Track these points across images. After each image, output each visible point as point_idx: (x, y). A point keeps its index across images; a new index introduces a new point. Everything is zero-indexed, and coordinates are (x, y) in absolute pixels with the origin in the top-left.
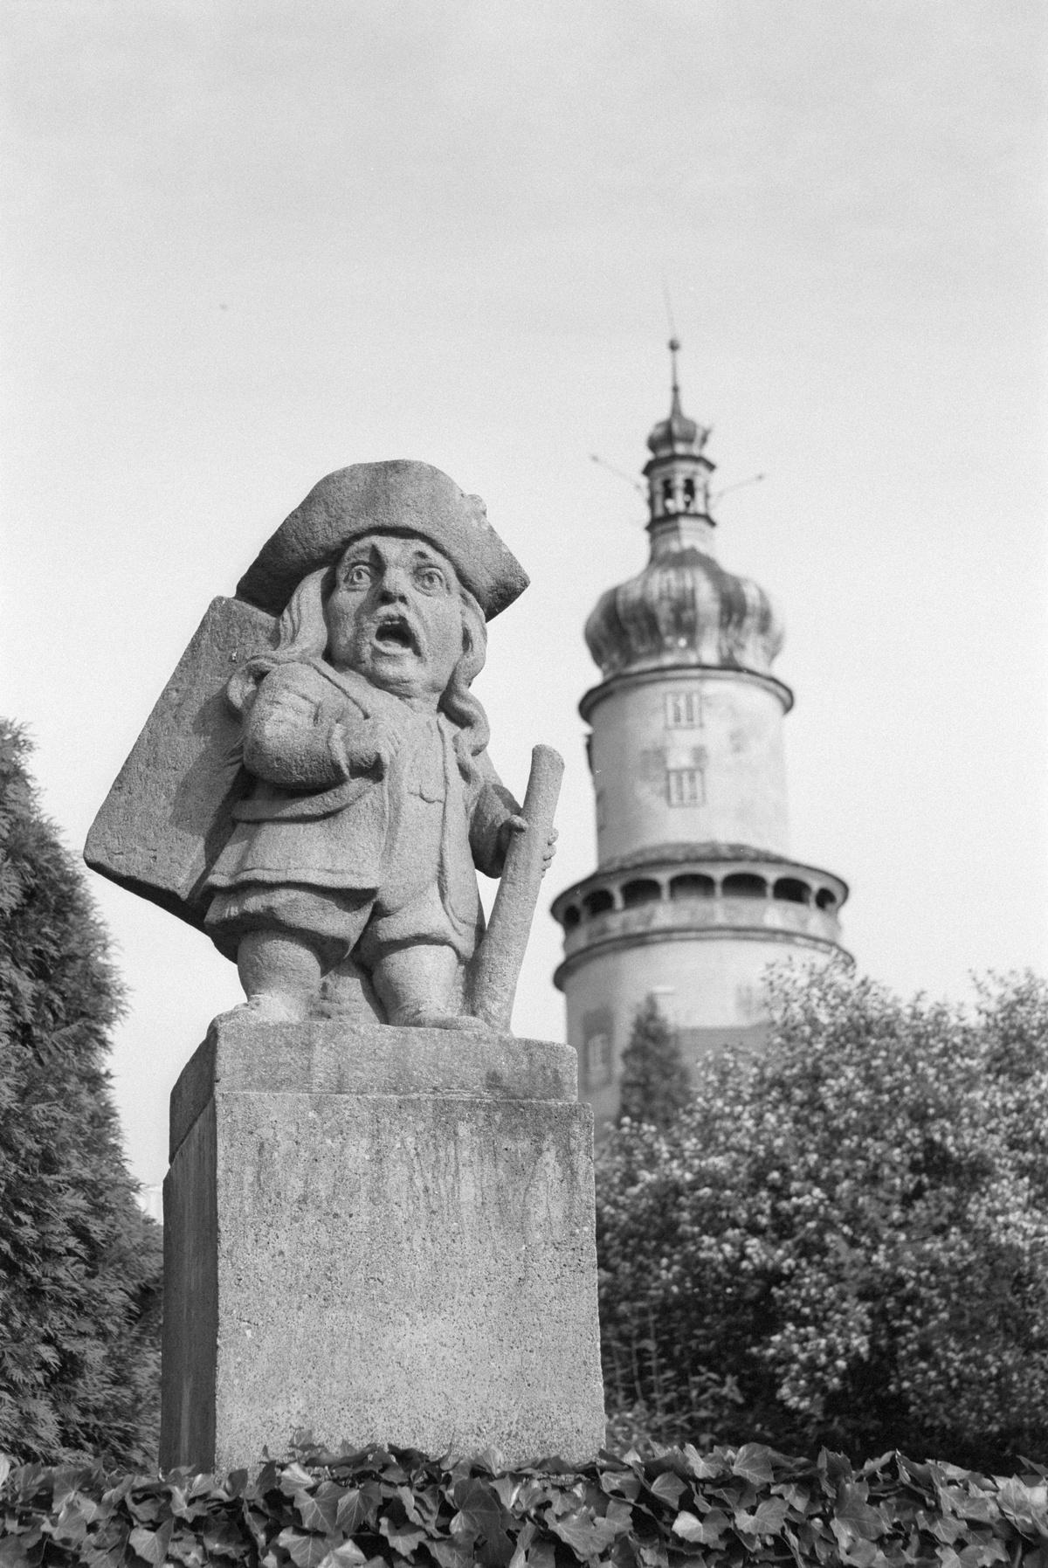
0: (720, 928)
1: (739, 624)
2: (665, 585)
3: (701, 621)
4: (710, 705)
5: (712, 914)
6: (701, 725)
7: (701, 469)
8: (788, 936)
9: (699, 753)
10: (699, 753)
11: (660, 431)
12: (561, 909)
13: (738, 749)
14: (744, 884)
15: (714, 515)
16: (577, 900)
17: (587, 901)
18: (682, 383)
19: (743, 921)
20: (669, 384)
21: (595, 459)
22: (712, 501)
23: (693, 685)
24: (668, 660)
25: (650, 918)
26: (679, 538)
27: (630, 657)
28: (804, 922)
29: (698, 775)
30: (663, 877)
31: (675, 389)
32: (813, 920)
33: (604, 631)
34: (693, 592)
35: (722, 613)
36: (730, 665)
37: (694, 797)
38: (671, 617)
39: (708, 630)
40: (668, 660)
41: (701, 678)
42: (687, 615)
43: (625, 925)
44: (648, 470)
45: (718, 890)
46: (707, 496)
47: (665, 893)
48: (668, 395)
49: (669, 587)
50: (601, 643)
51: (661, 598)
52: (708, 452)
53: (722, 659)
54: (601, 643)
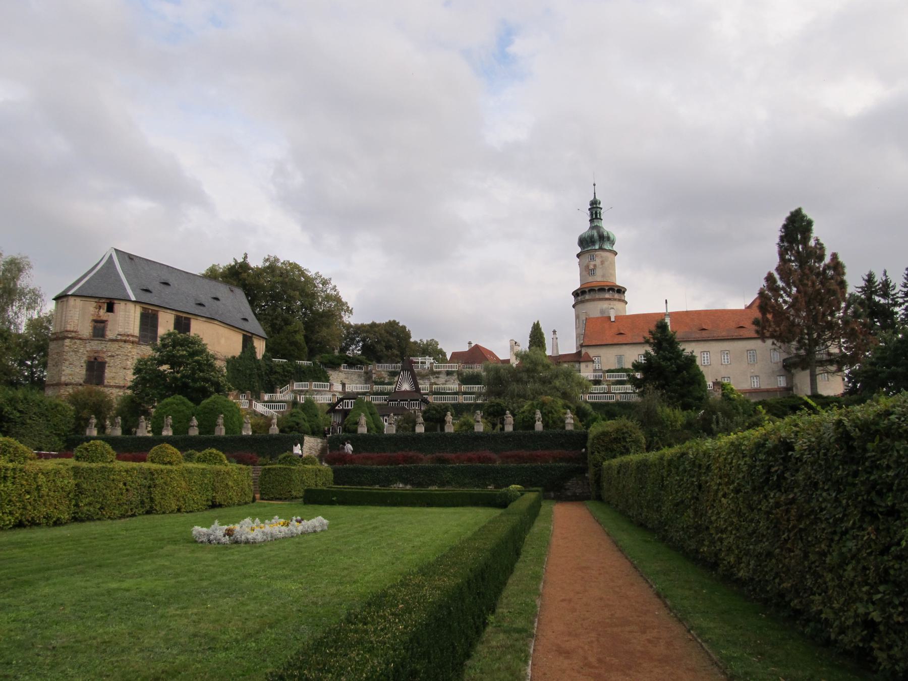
8: (610, 299)
9: (595, 266)
14: (602, 290)
19: (601, 297)
24: (589, 248)
25: (584, 298)
28: (614, 296)
30: (587, 290)
31: (595, 193)
32: (616, 296)
36: (601, 249)
40: (589, 248)
42: (593, 240)
52: (601, 206)
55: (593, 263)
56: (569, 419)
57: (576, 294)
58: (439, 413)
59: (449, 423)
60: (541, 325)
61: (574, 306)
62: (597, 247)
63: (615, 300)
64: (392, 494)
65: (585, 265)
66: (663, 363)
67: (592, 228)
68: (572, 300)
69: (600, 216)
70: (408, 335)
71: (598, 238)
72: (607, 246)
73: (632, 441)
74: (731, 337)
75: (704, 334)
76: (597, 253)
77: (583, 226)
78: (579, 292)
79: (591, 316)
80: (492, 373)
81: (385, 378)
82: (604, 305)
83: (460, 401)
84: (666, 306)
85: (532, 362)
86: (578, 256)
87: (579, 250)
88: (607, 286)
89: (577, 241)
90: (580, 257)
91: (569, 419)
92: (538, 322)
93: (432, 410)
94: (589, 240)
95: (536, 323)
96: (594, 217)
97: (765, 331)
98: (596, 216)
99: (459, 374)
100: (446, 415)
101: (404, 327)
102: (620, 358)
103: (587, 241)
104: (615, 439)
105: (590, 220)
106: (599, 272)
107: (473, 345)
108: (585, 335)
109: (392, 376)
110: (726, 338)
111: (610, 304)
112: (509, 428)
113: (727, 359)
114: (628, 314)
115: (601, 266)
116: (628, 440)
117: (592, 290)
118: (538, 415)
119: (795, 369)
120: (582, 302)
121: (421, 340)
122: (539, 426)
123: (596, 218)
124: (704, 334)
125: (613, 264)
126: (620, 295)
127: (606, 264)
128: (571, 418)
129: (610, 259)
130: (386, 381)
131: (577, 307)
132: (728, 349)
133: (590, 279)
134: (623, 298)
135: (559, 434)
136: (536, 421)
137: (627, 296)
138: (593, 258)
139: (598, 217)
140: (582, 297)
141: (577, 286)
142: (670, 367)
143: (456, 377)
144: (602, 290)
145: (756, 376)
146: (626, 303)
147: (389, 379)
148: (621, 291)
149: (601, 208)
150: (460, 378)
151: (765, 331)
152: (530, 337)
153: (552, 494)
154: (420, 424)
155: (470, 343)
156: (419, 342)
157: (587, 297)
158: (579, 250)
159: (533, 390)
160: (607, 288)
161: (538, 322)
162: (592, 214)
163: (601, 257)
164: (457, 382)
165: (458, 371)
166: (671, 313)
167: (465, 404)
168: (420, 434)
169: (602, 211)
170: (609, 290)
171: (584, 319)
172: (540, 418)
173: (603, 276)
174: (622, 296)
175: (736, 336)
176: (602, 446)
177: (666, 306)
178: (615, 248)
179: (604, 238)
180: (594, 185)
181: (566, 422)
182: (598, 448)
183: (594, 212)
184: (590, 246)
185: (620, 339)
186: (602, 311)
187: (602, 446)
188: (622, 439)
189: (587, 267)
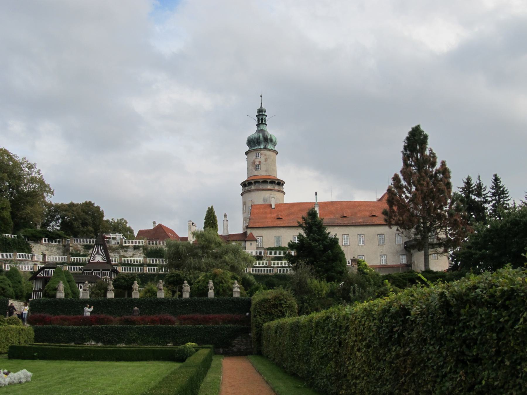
0: (261, 189)
1: (267, 141)
7: (264, 116)
8: (271, 190)
9: (260, 162)
10: (260, 162)
13: (266, 161)
14: (265, 182)
15: (267, 124)
16: (243, 185)
17: (244, 185)
18: (262, 102)
19: (264, 188)
22: (266, 121)
23: (259, 152)
24: (256, 148)
25: (251, 187)
27: (251, 147)
30: (253, 182)
31: (261, 103)
32: (277, 187)
36: (265, 148)
37: (259, 169)
39: (262, 143)
40: (256, 148)
41: (261, 151)
42: (258, 141)
52: (266, 114)
53: (264, 147)
55: (258, 160)
56: (236, 288)
57: (244, 185)
58: (127, 281)
59: (136, 290)
60: (214, 210)
61: (242, 195)
62: (262, 147)
63: (276, 190)
64: (87, 351)
66: (313, 244)
67: (258, 131)
68: (240, 190)
69: (265, 122)
70: (101, 215)
72: (270, 147)
73: (287, 307)
74: (366, 224)
75: (345, 221)
76: (262, 152)
77: (252, 130)
78: (246, 183)
79: (256, 203)
80: (173, 249)
81: (80, 251)
82: (267, 195)
83: (145, 272)
84: (316, 197)
85: (206, 240)
86: (247, 153)
87: (247, 148)
88: (269, 179)
89: (246, 141)
90: (248, 155)
91: (236, 288)
92: (212, 207)
93: (121, 279)
94: (255, 141)
95: (210, 207)
96: (260, 122)
97: (392, 220)
98: (262, 121)
99: (145, 248)
100: (133, 283)
101: (98, 208)
102: (278, 238)
103: (254, 141)
104: (273, 305)
105: (257, 125)
106: (263, 167)
107: (157, 225)
108: (250, 219)
109: (87, 249)
110: (362, 224)
111: (271, 194)
112: (186, 295)
113: (363, 241)
114: (285, 202)
115: (264, 163)
116: (284, 306)
117: (257, 182)
118: (211, 284)
119: (414, 250)
120: (249, 191)
121: (112, 219)
122: (211, 294)
123: (262, 123)
124: (345, 221)
125: (274, 161)
126: (279, 187)
127: (269, 161)
128: (238, 287)
130: (81, 254)
131: (244, 195)
132: (363, 233)
133: (256, 173)
134: (282, 190)
135: (228, 300)
136: (209, 290)
137: (285, 188)
138: (258, 156)
139: (264, 122)
140: (249, 187)
141: (245, 178)
142: (318, 247)
143: (142, 251)
144: (265, 182)
145: (384, 255)
146: (284, 193)
147: (84, 251)
148: (280, 183)
149: (266, 116)
150: (145, 252)
151: (392, 220)
152: (205, 219)
153: (221, 350)
154: (111, 290)
155: (154, 223)
156: (111, 220)
157: (253, 187)
158: (247, 148)
159: (207, 263)
160: (269, 181)
161: (212, 207)
162: (258, 120)
164: (143, 255)
165: (143, 246)
166: (319, 203)
167: (149, 274)
168: (111, 299)
169: (267, 118)
171: (250, 205)
172: (212, 287)
173: (266, 171)
174: (281, 187)
175: (370, 223)
176: (263, 310)
177: (316, 197)
178: (276, 149)
179: (267, 140)
180: (261, 96)
181: (234, 290)
182: (260, 312)
183: (260, 118)
184: (256, 146)
185: (279, 223)
186: (265, 200)
187: (263, 310)
188: (279, 305)
189: (254, 162)
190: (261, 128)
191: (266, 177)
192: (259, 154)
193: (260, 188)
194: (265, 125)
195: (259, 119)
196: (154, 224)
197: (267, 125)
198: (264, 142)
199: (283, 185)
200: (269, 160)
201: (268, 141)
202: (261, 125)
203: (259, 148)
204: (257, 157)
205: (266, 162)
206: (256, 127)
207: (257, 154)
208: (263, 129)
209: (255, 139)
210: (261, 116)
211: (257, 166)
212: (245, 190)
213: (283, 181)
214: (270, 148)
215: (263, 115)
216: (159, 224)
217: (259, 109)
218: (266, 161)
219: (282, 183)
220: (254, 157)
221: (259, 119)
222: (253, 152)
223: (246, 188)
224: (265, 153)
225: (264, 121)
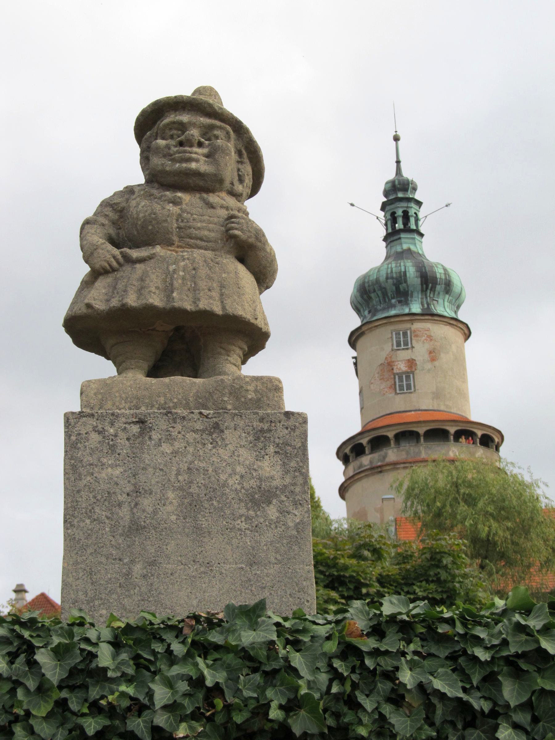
1: (433, 289)
2: (389, 271)
3: (411, 289)
4: (416, 336)
5: (420, 452)
6: (413, 347)
7: (412, 205)
9: (411, 363)
11: (389, 185)
12: (341, 455)
15: (422, 230)
16: (347, 450)
17: (353, 449)
18: (401, 159)
20: (395, 159)
21: (352, 205)
22: (420, 223)
23: (408, 325)
25: (385, 457)
26: (401, 244)
27: (374, 312)
28: (473, 454)
29: (411, 375)
30: (391, 434)
31: (398, 162)
33: (359, 299)
34: (405, 273)
35: (422, 284)
37: (409, 387)
38: (394, 288)
39: (415, 294)
40: (393, 312)
41: (412, 321)
42: (402, 287)
43: (371, 462)
44: (384, 207)
45: (422, 439)
46: (417, 220)
47: (392, 442)
48: (395, 165)
49: (392, 272)
50: (359, 306)
51: (387, 278)
54: (359, 306)
55: (404, 355)
65: (381, 360)
69: (417, 224)
71: (418, 281)
76: (417, 326)
88: (454, 422)
94: (390, 286)
96: (399, 225)
107: (29, 597)
115: (429, 366)
123: (407, 229)
125: (460, 360)
127: (445, 359)
129: (454, 347)
131: (356, 489)
149: (419, 204)
158: (355, 322)
160: (452, 430)
162: (393, 219)
163: (430, 338)
170: (458, 435)
180: (396, 139)
183: (399, 213)
184: (393, 306)
189: (389, 365)
190: (405, 247)
191: (438, 416)
192: (405, 334)
193: (418, 458)
194: (417, 237)
195: (393, 214)
196: (20, 596)
197: (422, 235)
198: (422, 291)
199: (497, 449)
200: (442, 355)
201: (438, 288)
202: (403, 235)
203: (407, 311)
204: (398, 344)
205: (436, 363)
206: (384, 244)
207: (398, 334)
208: (413, 248)
209: (390, 281)
210: (404, 204)
211: (401, 380)
212: (361, 466)
213: (499, 432)
214: (445, 314)
215: (409, 200)
216: (38, 593)
217: (393, 182)
218: (433, 360)
219: (496, 440)
220: (388, 348)
221: (393, 214)
222: (378, 331)
223: (366, 460)
224: (428, 330)
225: (412, 220)
